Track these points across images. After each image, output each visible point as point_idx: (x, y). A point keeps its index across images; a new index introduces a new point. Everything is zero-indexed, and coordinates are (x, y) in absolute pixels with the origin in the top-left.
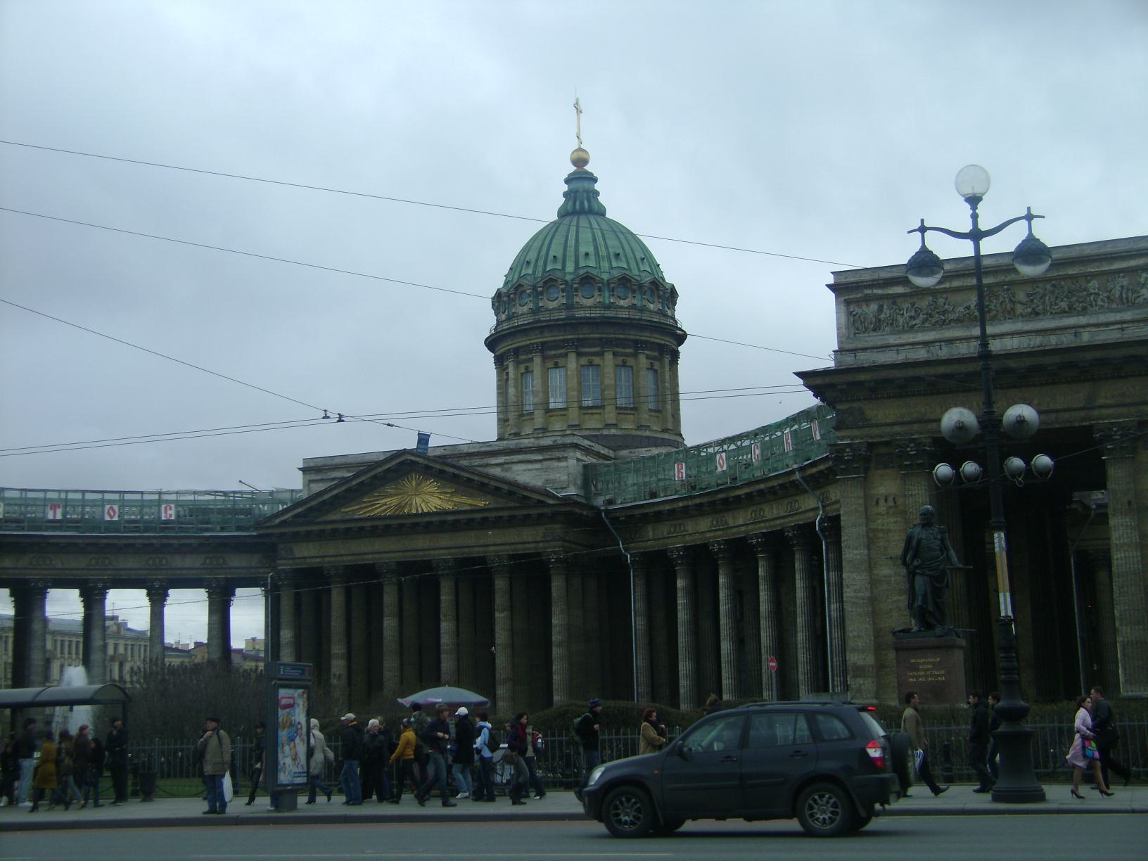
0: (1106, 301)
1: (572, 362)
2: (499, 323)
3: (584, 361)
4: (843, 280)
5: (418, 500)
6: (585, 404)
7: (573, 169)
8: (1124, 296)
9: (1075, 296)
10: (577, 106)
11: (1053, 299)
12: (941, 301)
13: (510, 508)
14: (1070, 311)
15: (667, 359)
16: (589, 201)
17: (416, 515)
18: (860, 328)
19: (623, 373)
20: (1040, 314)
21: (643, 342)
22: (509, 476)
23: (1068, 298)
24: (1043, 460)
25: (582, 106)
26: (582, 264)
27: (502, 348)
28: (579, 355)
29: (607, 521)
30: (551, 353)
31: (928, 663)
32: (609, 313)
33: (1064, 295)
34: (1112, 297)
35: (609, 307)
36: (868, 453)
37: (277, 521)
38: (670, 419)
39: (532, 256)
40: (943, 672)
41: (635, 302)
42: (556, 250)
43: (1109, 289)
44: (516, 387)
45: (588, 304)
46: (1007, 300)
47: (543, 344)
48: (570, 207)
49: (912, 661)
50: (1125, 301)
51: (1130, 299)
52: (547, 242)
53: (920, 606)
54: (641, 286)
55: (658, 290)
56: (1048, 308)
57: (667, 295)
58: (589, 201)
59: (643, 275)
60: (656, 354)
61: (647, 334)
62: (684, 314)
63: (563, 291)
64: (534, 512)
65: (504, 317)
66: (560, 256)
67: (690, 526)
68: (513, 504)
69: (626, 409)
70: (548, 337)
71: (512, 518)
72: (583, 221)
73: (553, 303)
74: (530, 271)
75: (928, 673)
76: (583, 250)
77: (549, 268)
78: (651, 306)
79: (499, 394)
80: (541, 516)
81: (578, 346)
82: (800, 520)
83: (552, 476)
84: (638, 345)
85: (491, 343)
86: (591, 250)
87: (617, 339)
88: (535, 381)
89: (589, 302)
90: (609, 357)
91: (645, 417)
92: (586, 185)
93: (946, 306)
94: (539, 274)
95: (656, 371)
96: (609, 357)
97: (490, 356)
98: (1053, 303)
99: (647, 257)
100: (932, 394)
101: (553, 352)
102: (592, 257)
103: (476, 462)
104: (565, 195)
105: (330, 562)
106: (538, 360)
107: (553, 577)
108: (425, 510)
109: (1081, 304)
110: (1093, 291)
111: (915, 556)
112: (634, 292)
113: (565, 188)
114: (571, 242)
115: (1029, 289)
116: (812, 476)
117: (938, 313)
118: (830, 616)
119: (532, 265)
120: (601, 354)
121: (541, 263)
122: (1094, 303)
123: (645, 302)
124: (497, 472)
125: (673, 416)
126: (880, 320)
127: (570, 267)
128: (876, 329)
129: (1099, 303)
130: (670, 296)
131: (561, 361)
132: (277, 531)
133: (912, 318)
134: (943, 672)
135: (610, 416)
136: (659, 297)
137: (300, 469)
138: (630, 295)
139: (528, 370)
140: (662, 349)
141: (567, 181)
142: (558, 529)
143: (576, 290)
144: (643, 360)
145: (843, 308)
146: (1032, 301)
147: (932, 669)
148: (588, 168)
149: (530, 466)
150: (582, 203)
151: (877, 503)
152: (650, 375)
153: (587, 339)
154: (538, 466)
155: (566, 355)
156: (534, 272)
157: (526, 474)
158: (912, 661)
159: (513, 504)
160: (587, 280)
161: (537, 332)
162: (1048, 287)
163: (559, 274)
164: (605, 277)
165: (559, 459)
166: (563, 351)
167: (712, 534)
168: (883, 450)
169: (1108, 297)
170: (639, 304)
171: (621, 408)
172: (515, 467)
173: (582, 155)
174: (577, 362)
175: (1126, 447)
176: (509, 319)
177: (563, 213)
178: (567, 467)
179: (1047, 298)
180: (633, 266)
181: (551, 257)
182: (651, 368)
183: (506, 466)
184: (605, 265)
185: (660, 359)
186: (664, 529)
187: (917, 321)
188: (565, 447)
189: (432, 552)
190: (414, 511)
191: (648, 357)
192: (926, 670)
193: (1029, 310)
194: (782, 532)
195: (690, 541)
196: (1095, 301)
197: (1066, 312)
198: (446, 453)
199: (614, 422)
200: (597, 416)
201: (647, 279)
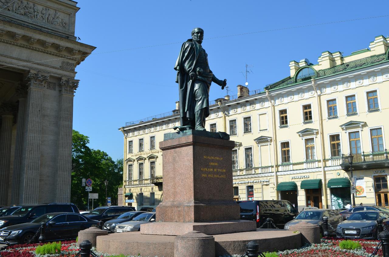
0: (41, 18)
9: (28, 9)
11: (17, 7)
14: (25, 14)
33: (24, 7)
34: (44, 17)
40: (224, 171)
43: (43, 13)
49: (205, 157)
51: (51, 21)
56: (14, 10)
75: (215, 170)
98: (17, 8)
109: (30, 14)
110: (37, 11)
122: (36, 16)
129: (38, 17)
169: (42, 17)
192: (214, 167)
196: (37, 16)
197: (22, 15)
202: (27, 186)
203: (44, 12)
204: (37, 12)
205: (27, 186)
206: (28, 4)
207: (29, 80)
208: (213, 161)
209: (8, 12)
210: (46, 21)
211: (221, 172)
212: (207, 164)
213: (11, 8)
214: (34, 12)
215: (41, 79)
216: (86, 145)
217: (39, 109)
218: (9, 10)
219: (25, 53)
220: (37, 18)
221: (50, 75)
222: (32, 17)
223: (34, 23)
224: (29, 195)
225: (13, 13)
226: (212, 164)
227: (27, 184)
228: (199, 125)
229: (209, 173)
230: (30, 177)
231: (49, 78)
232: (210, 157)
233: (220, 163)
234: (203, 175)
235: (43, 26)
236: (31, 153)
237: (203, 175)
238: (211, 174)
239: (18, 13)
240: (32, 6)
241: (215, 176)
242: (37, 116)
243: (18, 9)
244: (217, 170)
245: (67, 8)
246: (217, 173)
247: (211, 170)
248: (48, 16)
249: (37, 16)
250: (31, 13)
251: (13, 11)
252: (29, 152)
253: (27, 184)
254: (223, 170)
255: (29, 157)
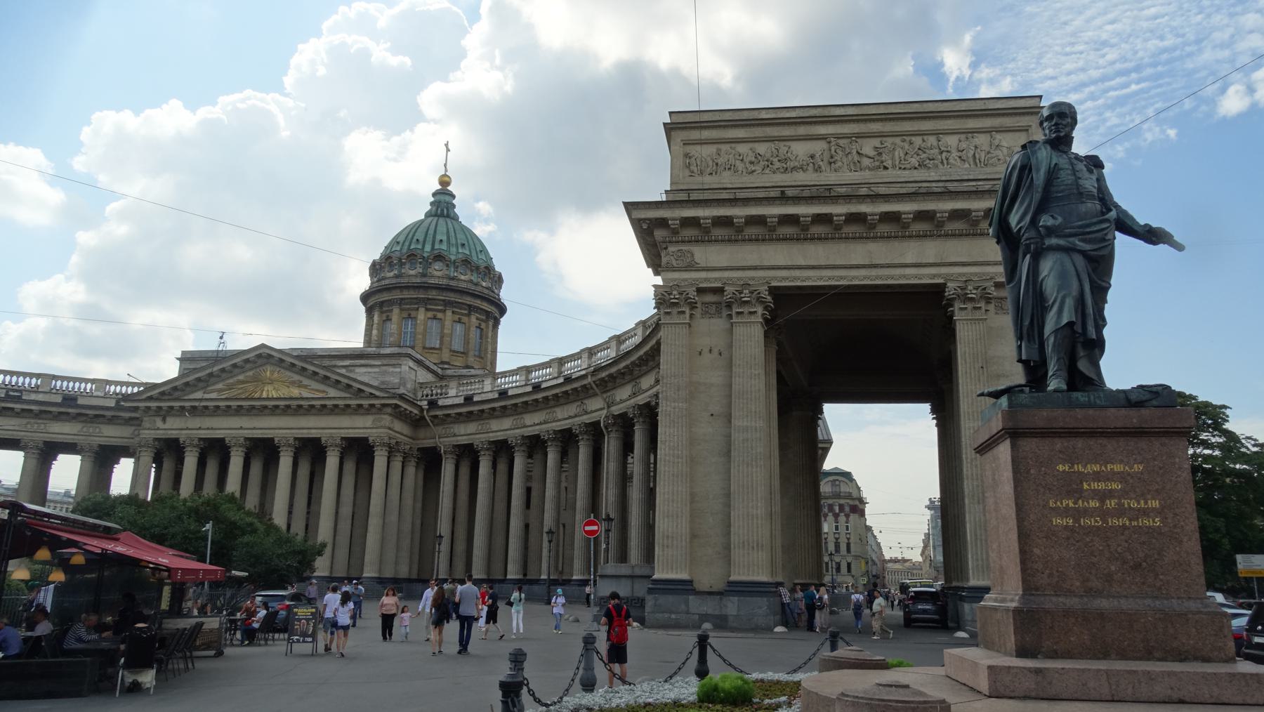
1: (421, 315)
2: (372, 283)
3: (430, 314)
4: (680, 119)
5: (270, 388)
6: (427, 346)
7: (439, 187)
8: (977, 156)
9: (925, 153)
10: (447, 145)
11: (902, 155)
12: (783, 149)
13: (345, 398)
14: (922, 165)
15: (491, 323)
16: (448, 210)
17: (268, 399)
18: (696, 171)
19: (459, 327)
20: (887, 168)
21: (475, 307)
22: (351, 375)
23: (918, 155)
24: (1172, 133)
25: (450, 147)
26: (437, 247)
27: (371, 302)
28: (427, 310)
29: (427, 418)
30: (409, 308)
31: (1109, 477)
32: (453, 283)
35: (453, 279)
36: (697, 298)
37: (144, 396)
38: (489, 363)
39: (401, 239)
40: (1155, 504)
41: (473, 278)
42: (419, 235)
44: (378, 330)
45: (438, 272)
46: (854, 152)
47: (402, 299)
48: (433, 213)
49: (1061, 468)
50: (978, 161)
51: (982, 160)
52: (413, 231)
53: (1070, 324)
54: (478, 268)
55: (490, 273)
56: (897, 163)
57: (496, 279)
58: (448, 210)
59: (481, 261)
60: (484, 318)
61: (479, 302)
62: (505, 295)
63: (420, 263)
64: (365, 402)
65: (375, 279)
66: (421, 240)
67: (495, 425)
68: (349, 396)
69: (458, 352)
70: (407, 294)
71: (348, 406)
72: (441, 221)
73: (412, 273)
74: (398, 248)
75: (1111, 504)
76: (439, 237)
77: (412, 247)
78: (484, 284)
79: (366, 335)
80: (372, 406)
81: (426, 302)
82: (587, 419)
83: (387, 379)
84: (471, 309)
85: (365, 298)
86: (445, 238)
87: (456, 302)
88: (393, 327)
89: (439, 274)
90: (449, 313)
91: (471, 360)
92: (447, 198)
93: (789, 154)
94: (405, 250)
95: (482, 329)
96: (449, 313)
97: (363, 308)
98: (902, 159)
99: (484, 250)
100: (771, 240)
101: (408, 306)
102: (445, 243)
103: (327, 363)
104: (432, 204)
105: (186, 434)
106: (396, 311)
107: (376, 458)
108: (275, 396)
110: (946, 149)
111: (1042, 208)
112: (472, 271)
113: (432, 199)
114: (431, 232)
115: (876, 142)
116: (602, 380)
117: (779, 161)
118: (606, 499)
119: (401, 244)
120: (444, 311)
121: (407, 244)
122: (945, 162)
123: (479, 280)
124: (343, 371)
125: (491, 364)
126: (717, 164)
127: (428, 248)
128: (711, 174)
129: (951, 161)
130: (499, 280)
131: (413, 314)
132: (141, 405)
133: (751, 163)
134: (1155, 504)
135: (446, 356)
136: (490, 278)
137: (177, 359)
138: (469, 273)
139: (389, 319)
140: (488, 314)
141: (434, 195)
142: (386, 420)
143: (430, 263)
144: (473, 319)
145: (678, 148)
146: (880, 154)
147: (1124, 494)
148: (449, 188)
149: (369, 370)
150: (442, 210)
151: (700, 353)
152: (478, 330)
153: (435, 299)
154: (377, 370)
155: (417, 309)
156: (401, 249)
157: (365, 375)
158: (1061, 468)
159: (349, 396)
160: (439, 257)
161: (398, 291)
162: (898, 140)
163: (419, 252)
164: (453, 258)
165: (394, 365)
166: (416, 306)
167: (512, 432)
168: (710, 298)
169: (960, 157)
170: (475, 280)
171: (454, 351)
172: (358, 370)
173: (447, 179)
174: (425, 315)
175: (980, 307)
176: (377, 281)
177: (428, 215)
178: (400, 372)
179: (897, 153)
180: (474, 254)
181: (414, 240)
182: (479, 327)
183: (350, 368)
184: (453, 250)
185: (486, 321)
186: (472, 427)
187: (757, 168)
188: (399, 355)
189: (277, 431)
190: (264, 395)
191: (477, 319)
192: (1103, 496)
193: (877, 163)
194: (570, 430)
195: (494, 437)
196: (947, 159)
197: (915, 168)
198: (302, 354)
199: (447, 360)
200: (436, 355)
201: (483, 265)
202: (976, 539)
203: (963, 145)
204: (948, 151)
205: (976, 539)
206: (924, 141)
207: (950, 303)
208: (1097, 477)
209: (885, 172)
210: (972, 163)
211: (1139, 510)
212: (1075, 486)
213: (889, 163)
214: (941, 153)
215: (974, 296)
216: (1224, 427)
217: (980, 365)
218: (885, 168)
219: (930, 250)
220: (948, 164)
221: (994, 283)
222: (937, 166)
223: (944, 178)
224: (982, 560)
225: (894, 172)
226: (1095, 485)
227: (976, 535)
228: (1053, 375)
229: (1086, 512)
230: (980, 520)
231: (993, 288)
232: (1085, 467)
233: (1131, 481)
234: (1058, 521)
235: (966, 178)
236: (976, 466)
237: (1058, 521)
238: (1092, 516)
239: (904, 169)
240: (935, 143)
241: (1115, 522)
242: (979, 380)
243: (905, 160)
244: (1120, 505)
245: (1018, 118)
246: (1120, 512)
247: (1094, 504)
248: (972, 152)
249: (947, 159)
250: (933, 159)
251: (894, 166)
252: (972, 464)
253: (976, 535)
254: (1146, 503)
255: (972, 475)
